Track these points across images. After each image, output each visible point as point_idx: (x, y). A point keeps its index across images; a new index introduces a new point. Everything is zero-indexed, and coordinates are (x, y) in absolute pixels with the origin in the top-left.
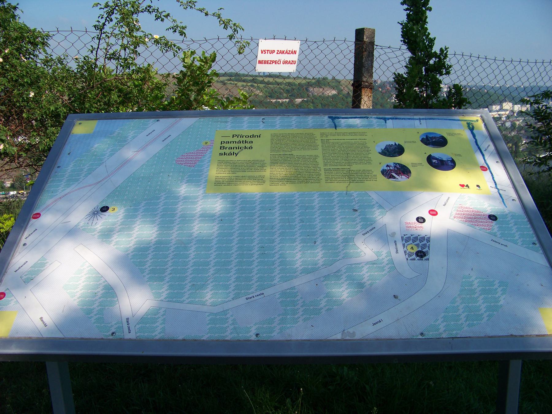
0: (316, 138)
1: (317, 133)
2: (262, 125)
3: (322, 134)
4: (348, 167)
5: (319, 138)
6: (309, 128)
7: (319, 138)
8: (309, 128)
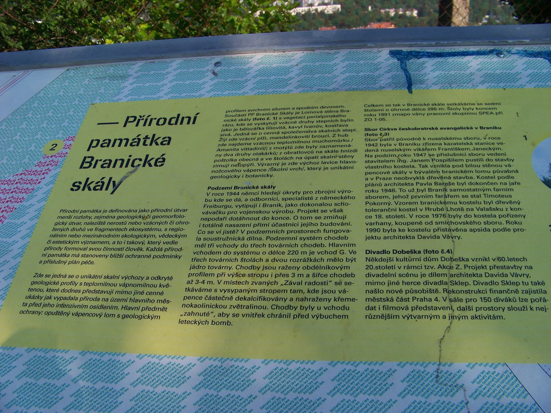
0: (351, 126)
1: (355, 104)
2: (209, 81)
3: (370, 110)
4: (446, 244)
5: (359, 122)
6: (334, 90)
7: (359, 122)
8: (334, 90)
